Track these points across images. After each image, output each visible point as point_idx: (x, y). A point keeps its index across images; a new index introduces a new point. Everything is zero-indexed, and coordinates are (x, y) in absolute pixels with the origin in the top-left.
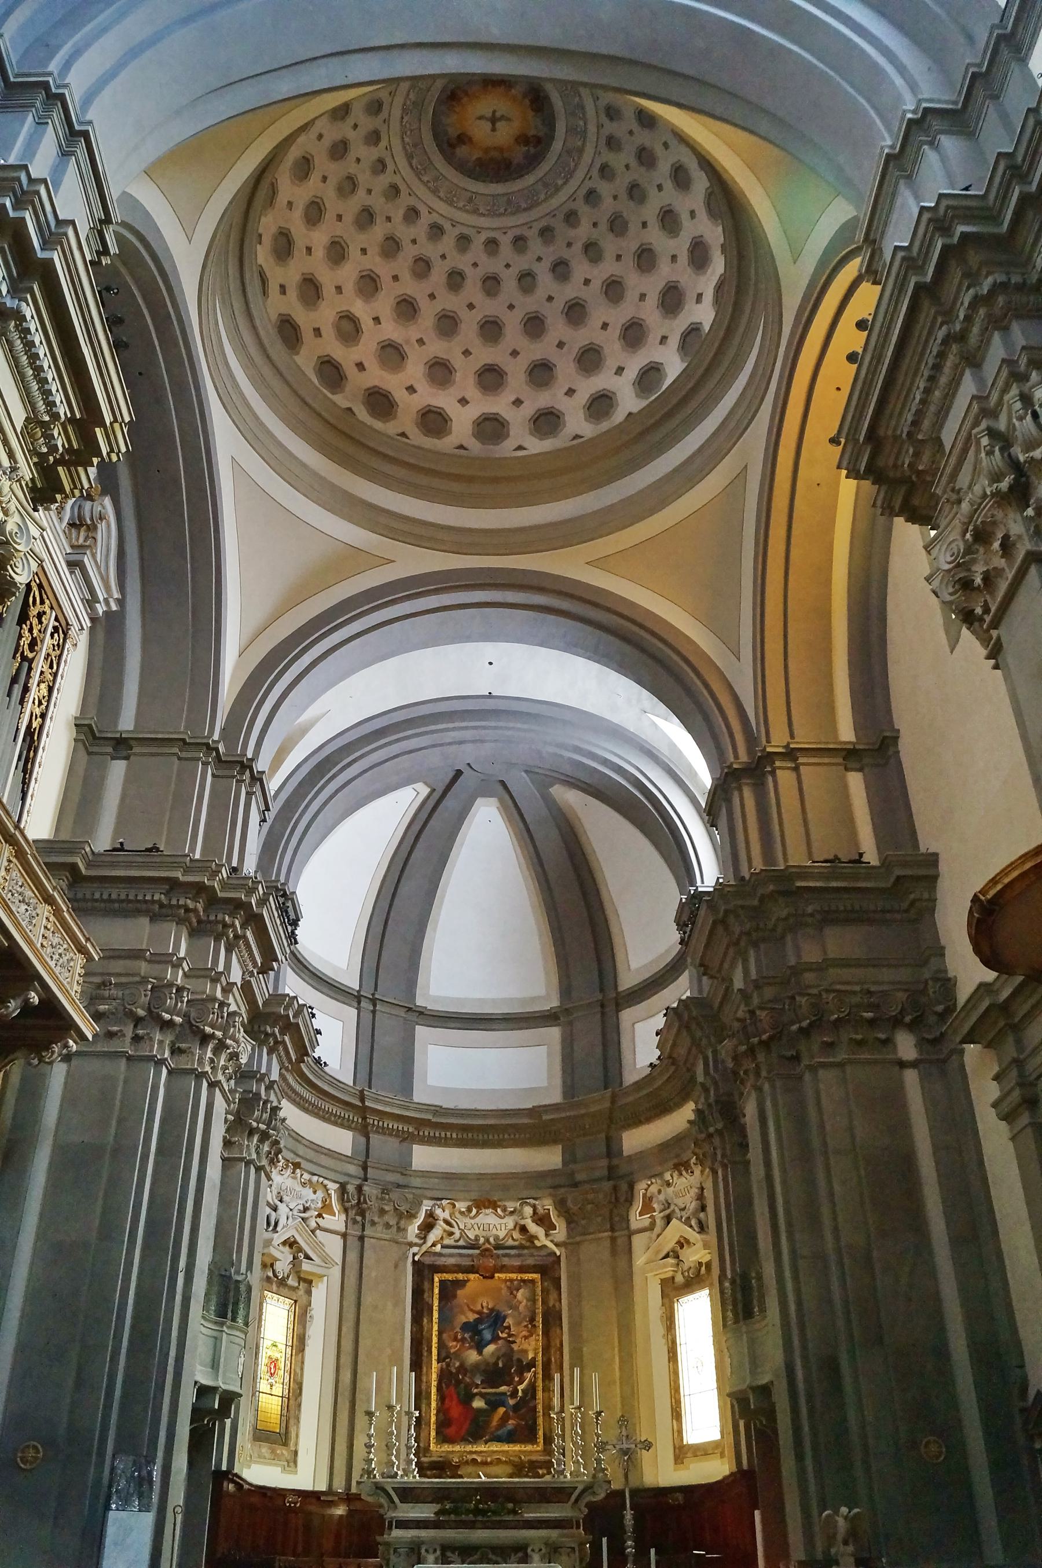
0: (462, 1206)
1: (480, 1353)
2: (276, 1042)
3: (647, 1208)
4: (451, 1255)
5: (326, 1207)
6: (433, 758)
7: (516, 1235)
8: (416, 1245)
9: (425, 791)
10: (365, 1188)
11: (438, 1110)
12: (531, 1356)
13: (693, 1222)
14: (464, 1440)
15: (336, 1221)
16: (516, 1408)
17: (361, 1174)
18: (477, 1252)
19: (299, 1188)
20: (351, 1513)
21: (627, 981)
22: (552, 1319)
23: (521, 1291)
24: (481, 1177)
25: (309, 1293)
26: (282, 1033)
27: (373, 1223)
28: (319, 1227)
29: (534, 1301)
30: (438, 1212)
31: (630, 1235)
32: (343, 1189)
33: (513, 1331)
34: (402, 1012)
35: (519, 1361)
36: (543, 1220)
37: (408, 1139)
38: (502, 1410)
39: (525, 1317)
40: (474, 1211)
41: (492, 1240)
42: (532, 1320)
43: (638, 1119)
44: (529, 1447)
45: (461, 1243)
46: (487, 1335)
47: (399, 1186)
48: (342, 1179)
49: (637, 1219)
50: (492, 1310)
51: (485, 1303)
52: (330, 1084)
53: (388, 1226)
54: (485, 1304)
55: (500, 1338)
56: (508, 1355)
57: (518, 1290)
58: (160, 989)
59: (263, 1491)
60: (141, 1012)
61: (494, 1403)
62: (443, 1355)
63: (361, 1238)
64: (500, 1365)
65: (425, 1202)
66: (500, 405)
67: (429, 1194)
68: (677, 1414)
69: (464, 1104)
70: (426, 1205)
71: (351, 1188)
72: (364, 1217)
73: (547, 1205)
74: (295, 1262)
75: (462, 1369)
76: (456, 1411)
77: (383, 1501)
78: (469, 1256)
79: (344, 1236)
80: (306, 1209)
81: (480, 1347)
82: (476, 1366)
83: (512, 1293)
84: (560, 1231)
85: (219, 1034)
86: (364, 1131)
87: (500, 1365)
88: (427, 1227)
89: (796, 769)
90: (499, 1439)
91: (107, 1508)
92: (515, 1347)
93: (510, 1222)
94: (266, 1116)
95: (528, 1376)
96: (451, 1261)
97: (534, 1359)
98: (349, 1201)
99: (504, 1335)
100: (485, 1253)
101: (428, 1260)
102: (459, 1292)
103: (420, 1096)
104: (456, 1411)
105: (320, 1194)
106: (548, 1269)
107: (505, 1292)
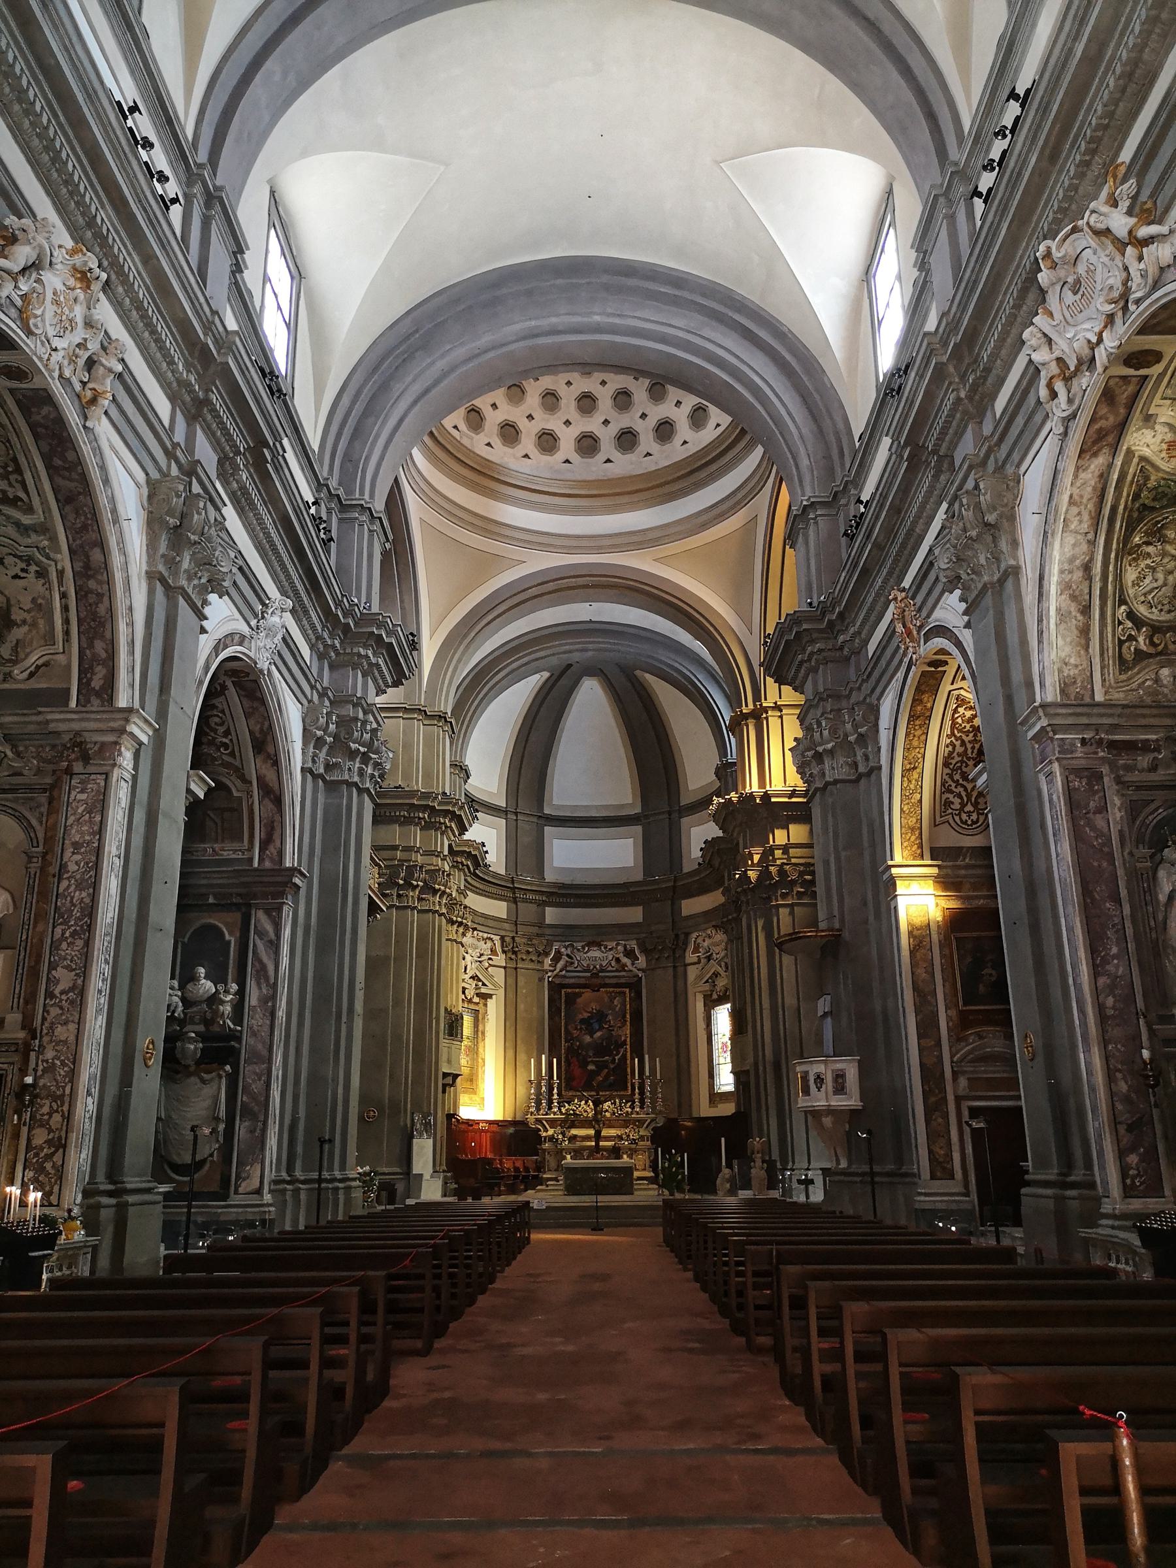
0: (579, 945)
1: (592, 1037)
2: (446, 827)
3: (696, 950)
5: (494, 952)
6: (554, 661)
7: (613, 963)
8: (550, 971)
9: (546, 675)
11: (564, 886)
12: (623, 1039)
13: (723, 964)
15: (500, 959)
17: (514, 929)
18: (589, 974)
19: (476, 942)
21: (684, 801)
22: (637, 1016)
25: (486, 1005)
26: (450, 821)
27: (523, 960)
28: (490, 965)
29: (625, 1006)
30: (563, 950)
31: (686, 965)
32: (502, 938)
34: (535, 820)
35: (616, 1041)
36: (629, 954)
37: (543, 904)
42: (624, 1016)
43: (690, 895)
45: (579, 969)
46: (596, 1026)
48: (503, 933)
49: (691, 957)
52: (493, 877)
58: (411, 870)
59: (469, 1123)
60: (401, 882)
61: (601, 1066)
63: (516, 969)
65: (555, 943)
66: (593, 425)
67: (557, 939)
68: (711, 1075)
69: (579, 880)
70: (556, 946)
71: (507, 939)
73: (633, 944)
75: (581, 1047)
76: (577, 1072)
79: (505, 968)
80: (482, 955)
82: (589, 1044)
84: (642, 961)
85: (443, 888)
86: (515, 901)
88: (556, 959)
89: (781, 717)
91: (412, 1137)
94: (461, 913)
96: (572, 981)
100: (595, 976)
101: (557, 981)
102: (579, 1000)
103: (549, 877)
104: (577, 1072)
105: (489, 944)
106: (635, 986)
107: (606, 999)
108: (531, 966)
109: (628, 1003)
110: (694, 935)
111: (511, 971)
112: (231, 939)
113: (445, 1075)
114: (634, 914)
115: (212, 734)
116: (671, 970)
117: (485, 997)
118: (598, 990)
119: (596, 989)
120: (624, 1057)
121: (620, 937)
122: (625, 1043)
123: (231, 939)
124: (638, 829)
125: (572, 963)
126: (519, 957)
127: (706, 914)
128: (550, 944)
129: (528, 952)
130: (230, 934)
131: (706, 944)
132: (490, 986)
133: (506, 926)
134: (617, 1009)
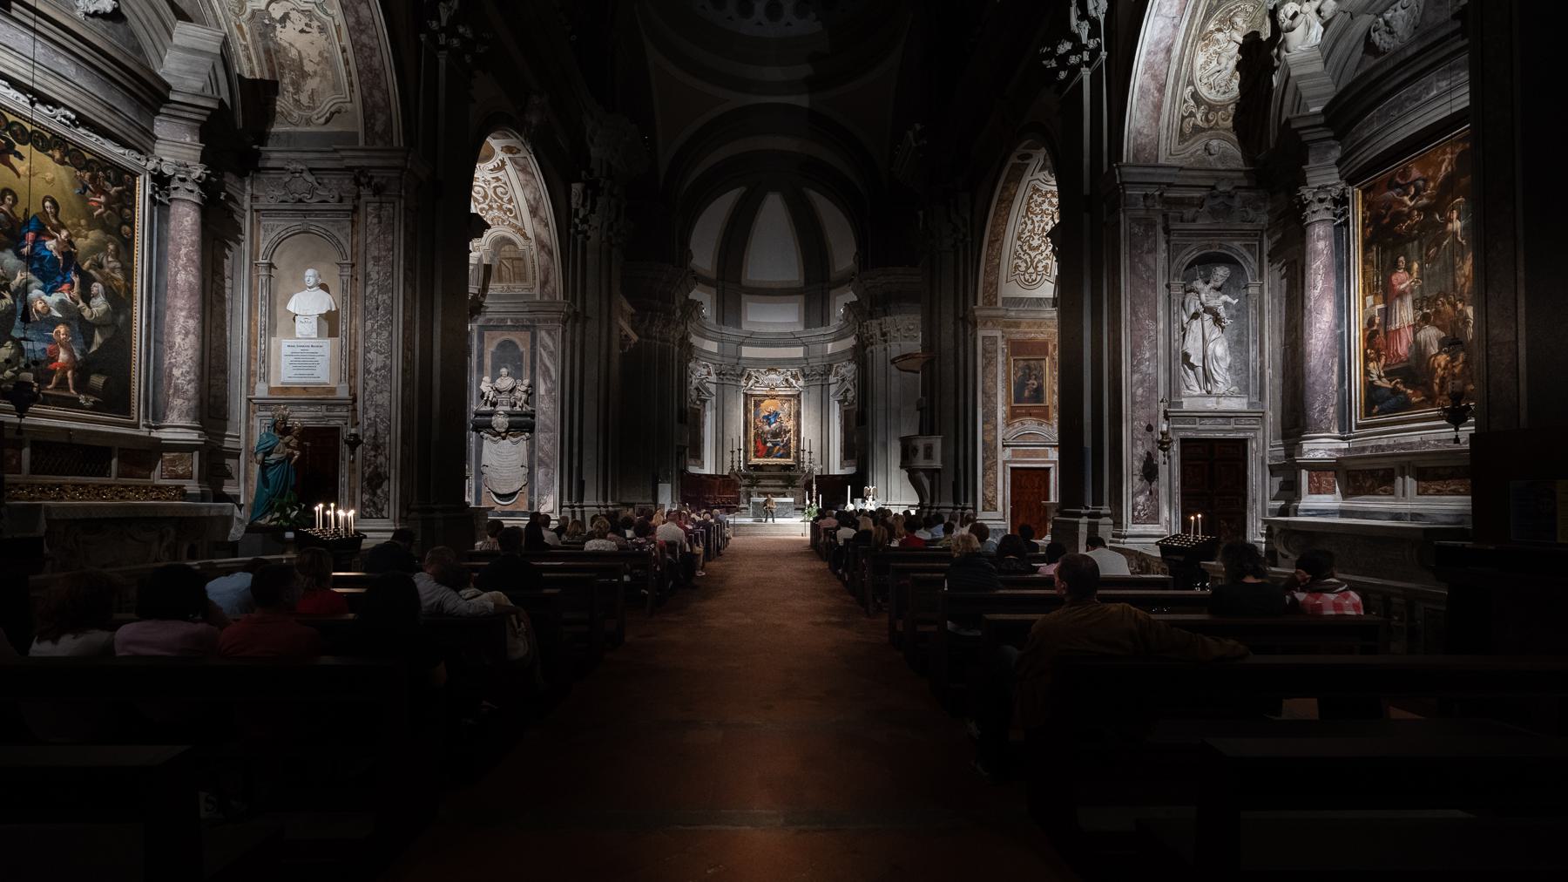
0: (763, 370)
3: (836, 375)
5: (709, 373)
14: (764, 457)
16: (783, 446)
20: (724, 481)
24: (771, 359)
25: (704, 406)
33: (783, 419)
36: (794, 377)
38: (778, 447)
46: (773, 420)
47: (737, 364)
51: (772, 409)
61: (775, 445)
74: (698, 396)
76: (761, 447)
77: (738, 479)
81: (769, 425)
82: (769, 431)
84: (801, 382)
90: (777, 457)
95: (788, 435)
96: (758, 393)
101: (749, 392)
104: (761, 447)
107: (780, 404)
110: (835, 366)
112: (524, 349)
113: (678, 447)
114: (798, 352)
115: (500, 201)
116: (820, 387)
117: (704, 401)
119: (773, 397)
120: (790, 439)
121: (788, 366)
122: (790, 431)
123: (524, 349)
124: (801, 298)
127: (843, 352)
128: (744, 369)
130: (525, 345)
131: (842, 371)
133: (718, 358)
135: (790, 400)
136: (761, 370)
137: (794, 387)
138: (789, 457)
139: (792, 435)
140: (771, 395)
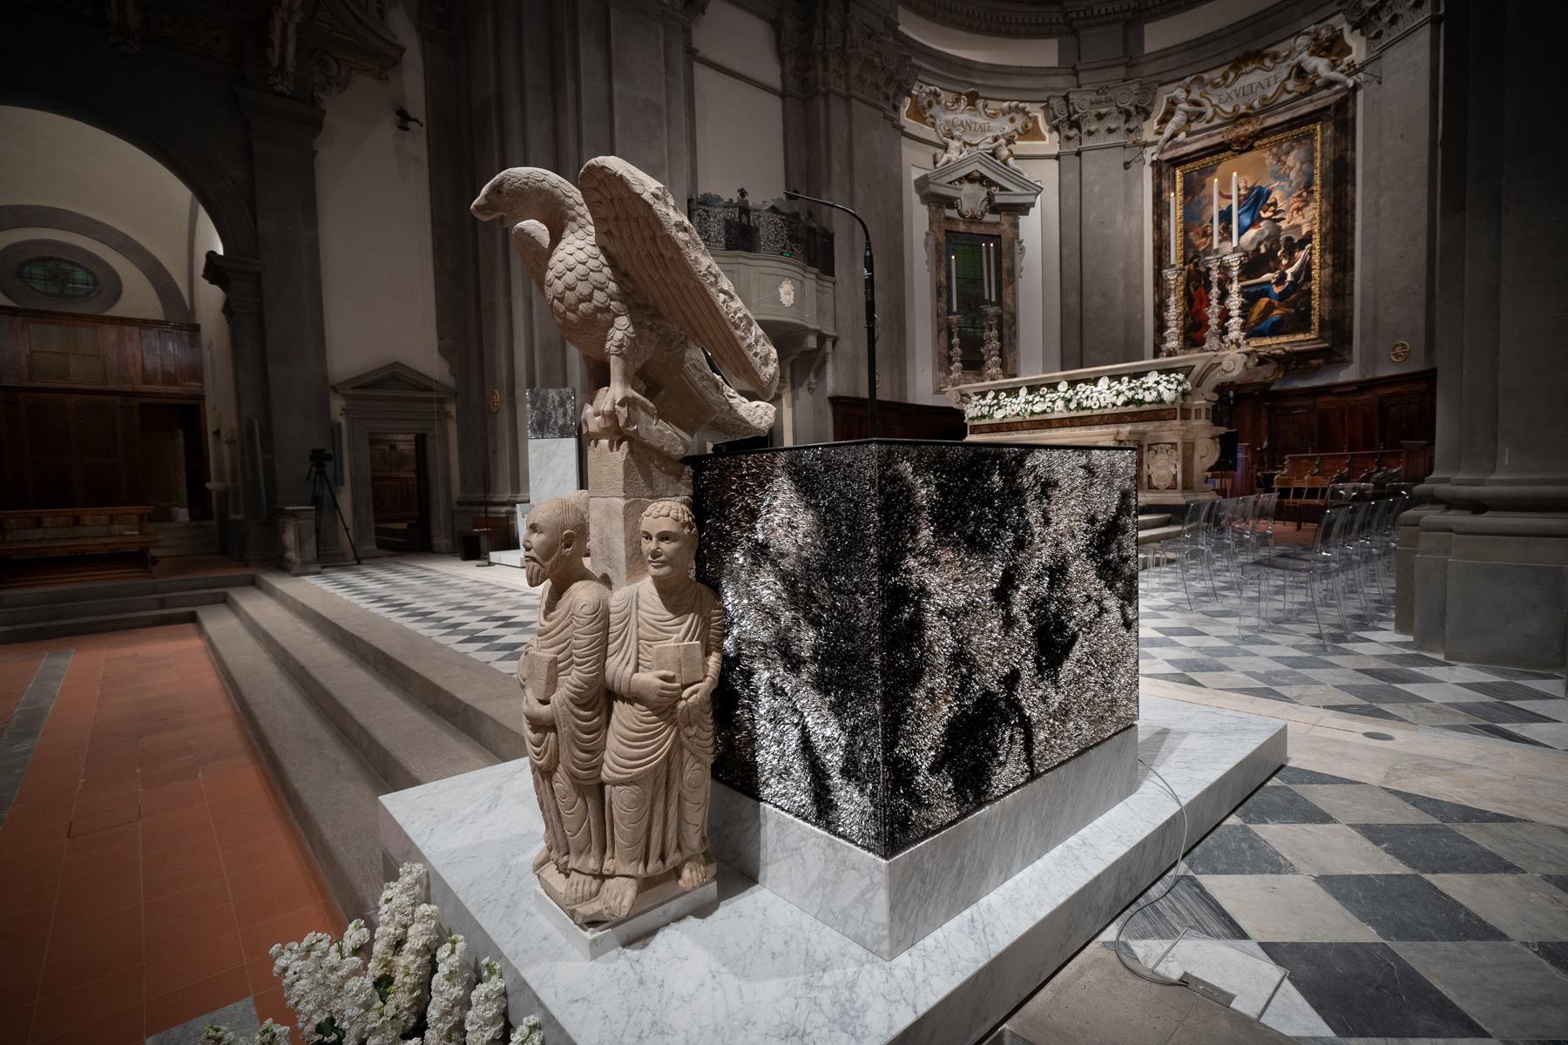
0: (1216, 75)
4: (1197, 141)
7: (1290, 85)
10: (1071, 96)
12: (1305, 230)
15: (1050, 143)
16: (1282, 296)
23: (1294, 153)
25: (1015, 225)
29: (1311, 161)
32: (1047, 107)
33: (1281, 205)
35: (1289, 239)
38: (1264, 301)
39: (1299, 184)
40: (1232, 75)
41: (1256, 104)
42: (1308, 187)
44: (1300, 337)
45: (1217, 121)
48: (1044, 96)
50: (1252, 189)
53: (1110, 131)
54: (1242, 185)
55: (1262, 219)
56: (1274, 237)
57: (1288, 153)
62: (1191, 255)
64: (1263, 250)
72: (1080, 129)
73: (1341, 23)
78: (1219, 133)
83: (1279, 161)
87: (1263, 250)
92: (1283, 225)
93: (1283, 71)
95: (1301, 255)
97: (1310, 233)
98: (1055, 117)
99: (1269, 214)
108: (1113, 139)
109: (1318, 155)
111: (1070, 158)
118: (1251, 148)
125: (1201, 114)
126: (1084, 129)
129: (1100, 117)
132: (1017, 190)
134: (1293, 175)
135: (1310, 136)
136: (1206, 76)
137: (1330, 84)
138: (1306, 328)
139: (1314, 252)
140: (1237, 140)
